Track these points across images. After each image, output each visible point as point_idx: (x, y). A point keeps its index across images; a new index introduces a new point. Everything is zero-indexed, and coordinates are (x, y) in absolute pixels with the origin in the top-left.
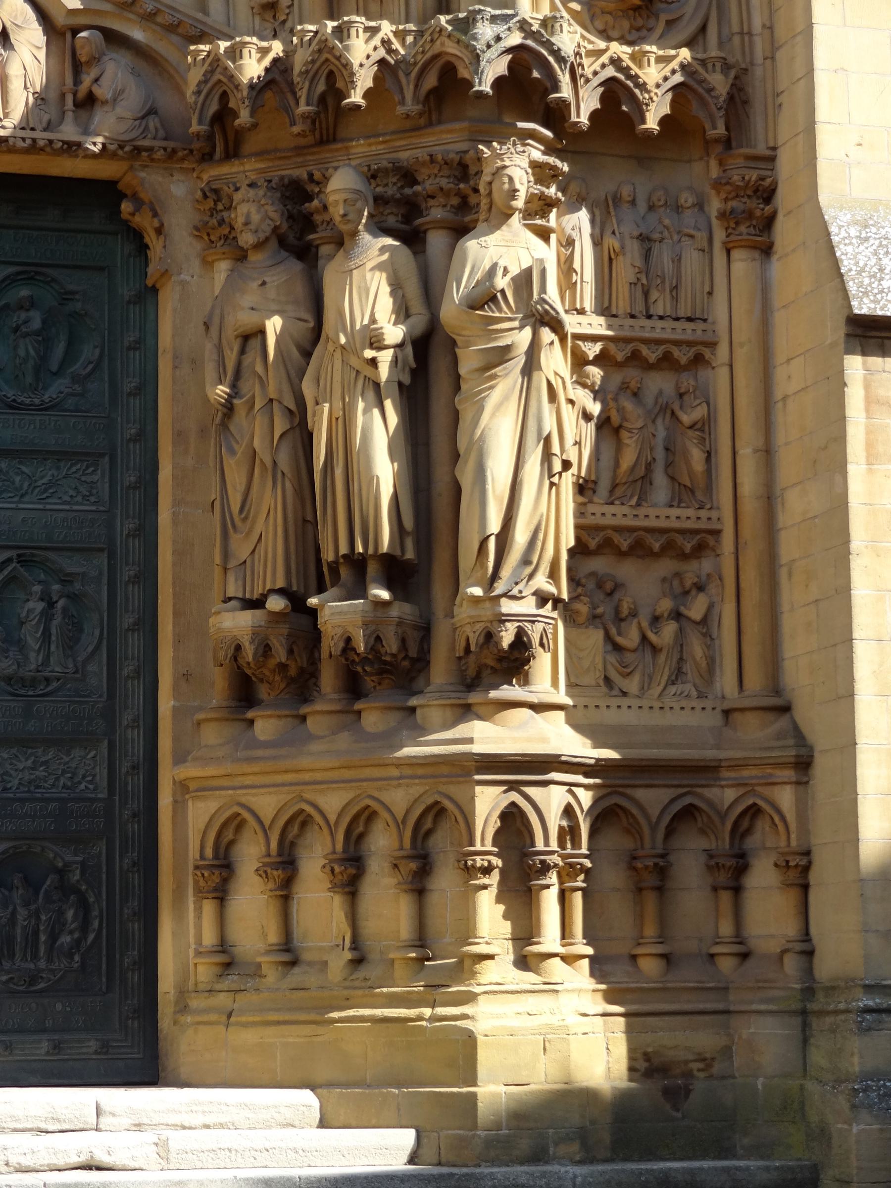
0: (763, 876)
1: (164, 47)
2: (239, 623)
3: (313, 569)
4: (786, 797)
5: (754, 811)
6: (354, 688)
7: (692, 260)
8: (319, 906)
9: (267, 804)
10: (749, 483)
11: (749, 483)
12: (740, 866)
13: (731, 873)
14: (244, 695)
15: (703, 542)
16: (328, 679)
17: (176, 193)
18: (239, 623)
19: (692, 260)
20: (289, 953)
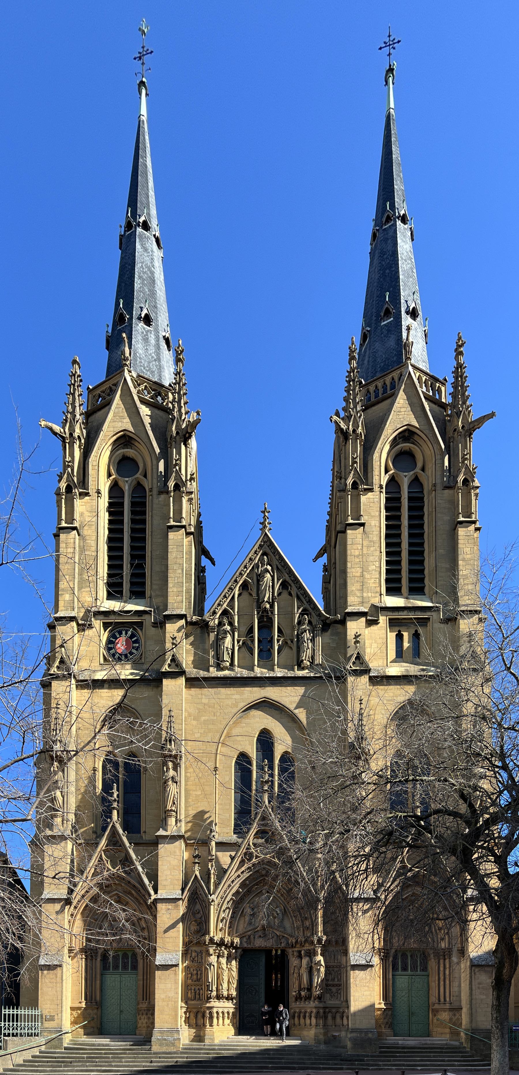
0: (345, 1018)
1: (289, 937)
2: (294, 993)
3: (300, 989)
4: (346, 1011)
5: (344, 1012)
6: (305, 1000)
7: (339, 957)
8: (302, 1020)
9: (298, 1010)
10: (344, 979)
11: (344, 979)
12: (343, 1017)
13: (342, 1018)
14: (296, 1000)
15: (340, 985)
16: (303, 999)
17: (290, 951)
18: (294, 993)
19: (339, 957)
20: (300, 1024)
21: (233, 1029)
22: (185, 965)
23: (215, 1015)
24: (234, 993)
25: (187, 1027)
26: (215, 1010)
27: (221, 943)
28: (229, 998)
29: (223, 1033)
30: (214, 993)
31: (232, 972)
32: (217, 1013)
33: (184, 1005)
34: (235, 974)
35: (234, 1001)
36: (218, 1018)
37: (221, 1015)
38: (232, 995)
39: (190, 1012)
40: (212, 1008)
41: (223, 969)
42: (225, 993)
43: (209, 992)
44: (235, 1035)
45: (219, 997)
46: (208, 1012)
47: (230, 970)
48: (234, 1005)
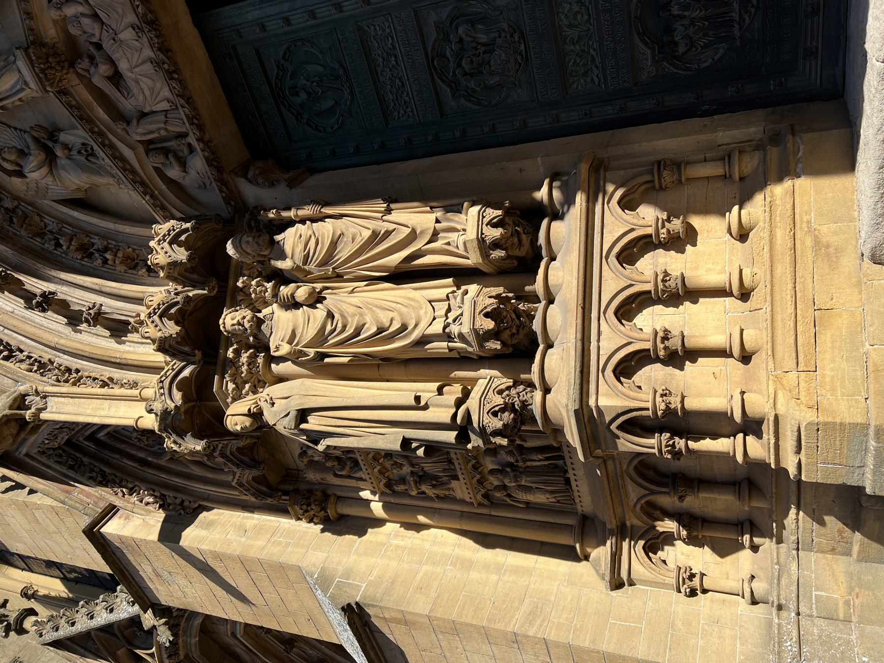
21: (778, 191)
22: (377, 508)
23: (651, 386)
24: (469, 229)
25: (767, 544)
26: (610, 398)
27: (198, 341)
28: (517, 262)
29: (821, 315)
30: (488, 386)
31: (344, 252)
32: (626, 368)
33: (602, 553)
34: (351, 226)
35: (542, 194)
36: (680, 356)
37: (651, 320)
38: (484, 246)
39: (656, 512)
40: (586, 417)
41: (321, 338)
42: (469, 309)
43: (475, 442)
44: (848, 164)
45: (514, 344)
46: (628, 443)
47: (332, 271)
48: (569, 201)
